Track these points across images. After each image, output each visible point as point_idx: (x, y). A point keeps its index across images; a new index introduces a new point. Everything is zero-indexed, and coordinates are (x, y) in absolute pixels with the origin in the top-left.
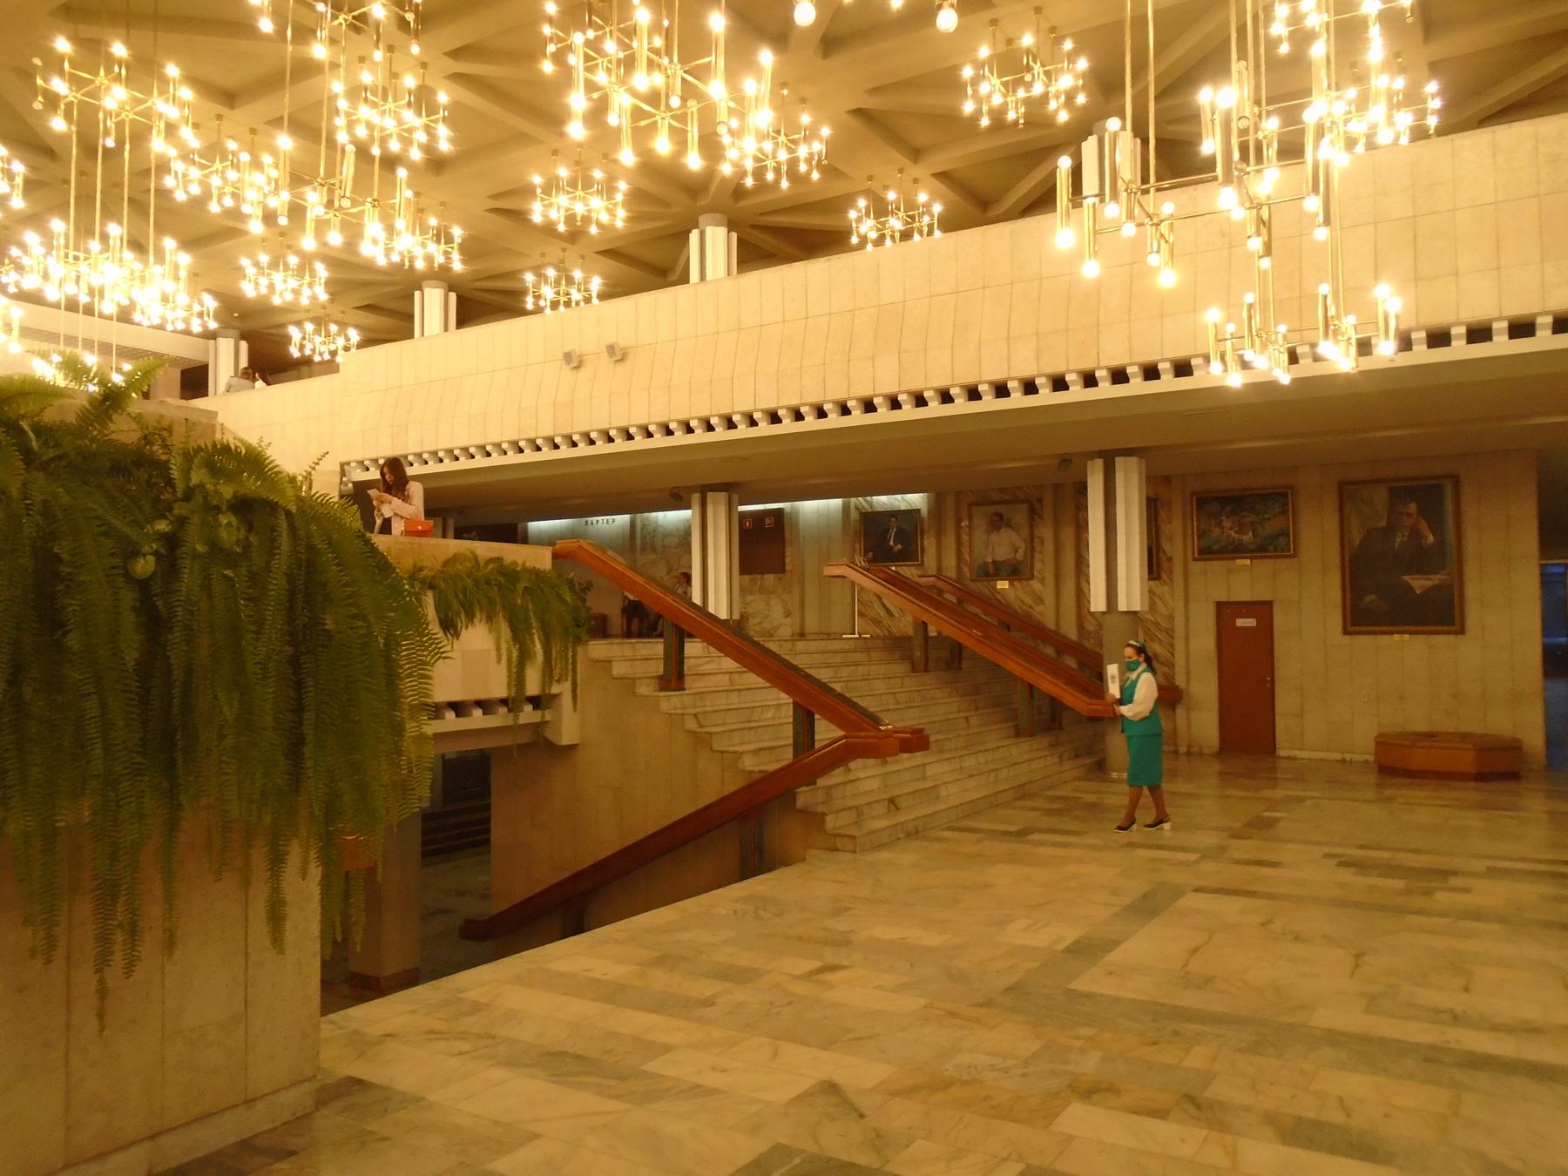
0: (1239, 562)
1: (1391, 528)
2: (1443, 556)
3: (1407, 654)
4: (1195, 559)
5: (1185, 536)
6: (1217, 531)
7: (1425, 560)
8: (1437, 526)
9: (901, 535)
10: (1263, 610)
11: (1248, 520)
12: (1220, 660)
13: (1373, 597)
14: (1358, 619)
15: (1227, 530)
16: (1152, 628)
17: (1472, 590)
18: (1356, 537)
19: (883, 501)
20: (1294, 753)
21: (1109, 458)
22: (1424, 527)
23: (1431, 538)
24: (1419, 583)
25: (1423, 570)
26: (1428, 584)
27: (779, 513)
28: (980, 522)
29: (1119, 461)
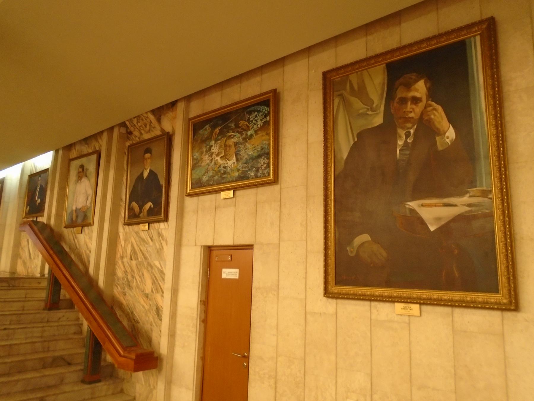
4: (188, 195)
6: (206, 158)
11: (231, 141)
12: (204, 321)
13: (365, 237)
14: (349, 273)
16: (158, 276)
18: (344, 145)
22: (439, 116)
23: (451, 134)
24: (433, 213)
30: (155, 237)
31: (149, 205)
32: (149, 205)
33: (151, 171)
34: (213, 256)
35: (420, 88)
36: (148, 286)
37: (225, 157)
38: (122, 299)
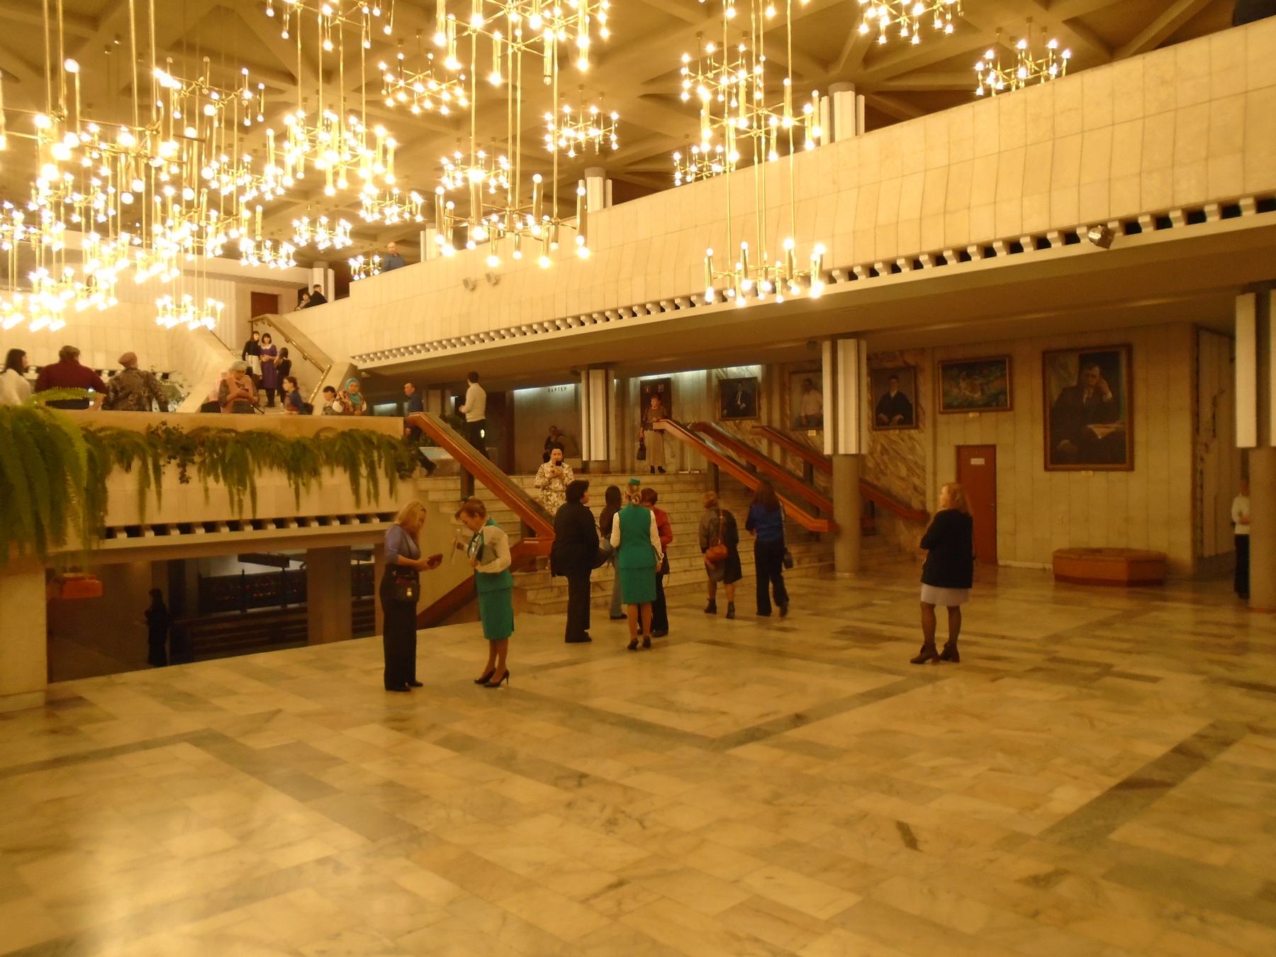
0: (971, 415)
1: (1079, 389)
2: (1119, 409)
3: (1091, 484)
5: (934, 391)
6: (956, 391)
7: (1107, 412)
8: (1114, 387)
9: (745, 397)
10: (989, 451)
11: (977, 382)
13: (1066, 441)
14: (1056, 459)
15: (963, 389)
17: (1140, 435)
18: (1055, 393)
19: (735, 371)
20: (1009, 563)
21: (834, 339)
22: (1104, 385)
23: (1110, 395)
24: (1100, 431)
25: (1102, 420)
26: (1107, 431)
27: (667, 382)
28: (797, 387)
29: (840, 342)
30: (906, 438)
31: (899, 417)
32: (899, 417)
33: (899, 394)
34: (963, 452)
35: (1096, 371)
36: (904, 472)
37: (973, 390)
38: (876, 482)
